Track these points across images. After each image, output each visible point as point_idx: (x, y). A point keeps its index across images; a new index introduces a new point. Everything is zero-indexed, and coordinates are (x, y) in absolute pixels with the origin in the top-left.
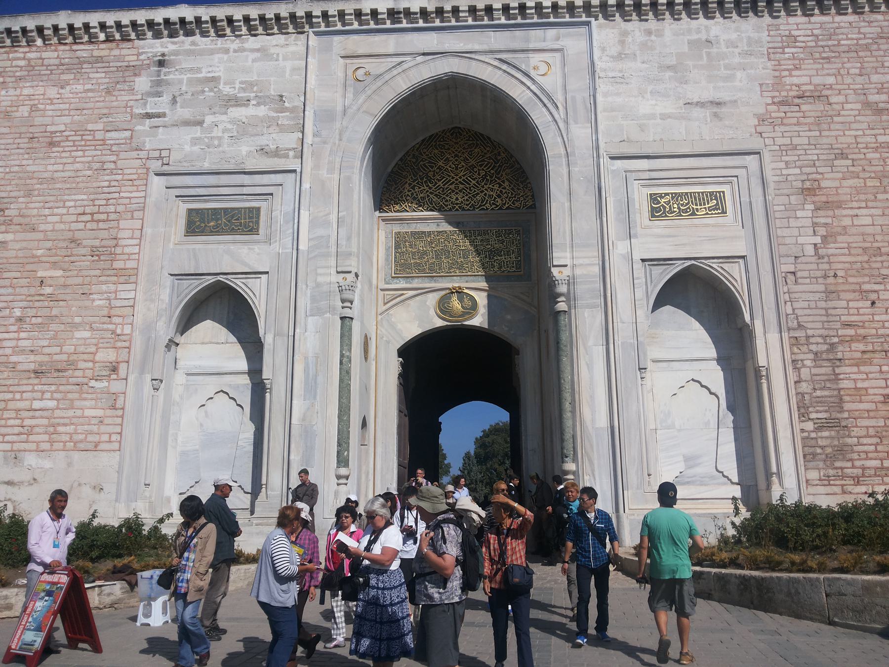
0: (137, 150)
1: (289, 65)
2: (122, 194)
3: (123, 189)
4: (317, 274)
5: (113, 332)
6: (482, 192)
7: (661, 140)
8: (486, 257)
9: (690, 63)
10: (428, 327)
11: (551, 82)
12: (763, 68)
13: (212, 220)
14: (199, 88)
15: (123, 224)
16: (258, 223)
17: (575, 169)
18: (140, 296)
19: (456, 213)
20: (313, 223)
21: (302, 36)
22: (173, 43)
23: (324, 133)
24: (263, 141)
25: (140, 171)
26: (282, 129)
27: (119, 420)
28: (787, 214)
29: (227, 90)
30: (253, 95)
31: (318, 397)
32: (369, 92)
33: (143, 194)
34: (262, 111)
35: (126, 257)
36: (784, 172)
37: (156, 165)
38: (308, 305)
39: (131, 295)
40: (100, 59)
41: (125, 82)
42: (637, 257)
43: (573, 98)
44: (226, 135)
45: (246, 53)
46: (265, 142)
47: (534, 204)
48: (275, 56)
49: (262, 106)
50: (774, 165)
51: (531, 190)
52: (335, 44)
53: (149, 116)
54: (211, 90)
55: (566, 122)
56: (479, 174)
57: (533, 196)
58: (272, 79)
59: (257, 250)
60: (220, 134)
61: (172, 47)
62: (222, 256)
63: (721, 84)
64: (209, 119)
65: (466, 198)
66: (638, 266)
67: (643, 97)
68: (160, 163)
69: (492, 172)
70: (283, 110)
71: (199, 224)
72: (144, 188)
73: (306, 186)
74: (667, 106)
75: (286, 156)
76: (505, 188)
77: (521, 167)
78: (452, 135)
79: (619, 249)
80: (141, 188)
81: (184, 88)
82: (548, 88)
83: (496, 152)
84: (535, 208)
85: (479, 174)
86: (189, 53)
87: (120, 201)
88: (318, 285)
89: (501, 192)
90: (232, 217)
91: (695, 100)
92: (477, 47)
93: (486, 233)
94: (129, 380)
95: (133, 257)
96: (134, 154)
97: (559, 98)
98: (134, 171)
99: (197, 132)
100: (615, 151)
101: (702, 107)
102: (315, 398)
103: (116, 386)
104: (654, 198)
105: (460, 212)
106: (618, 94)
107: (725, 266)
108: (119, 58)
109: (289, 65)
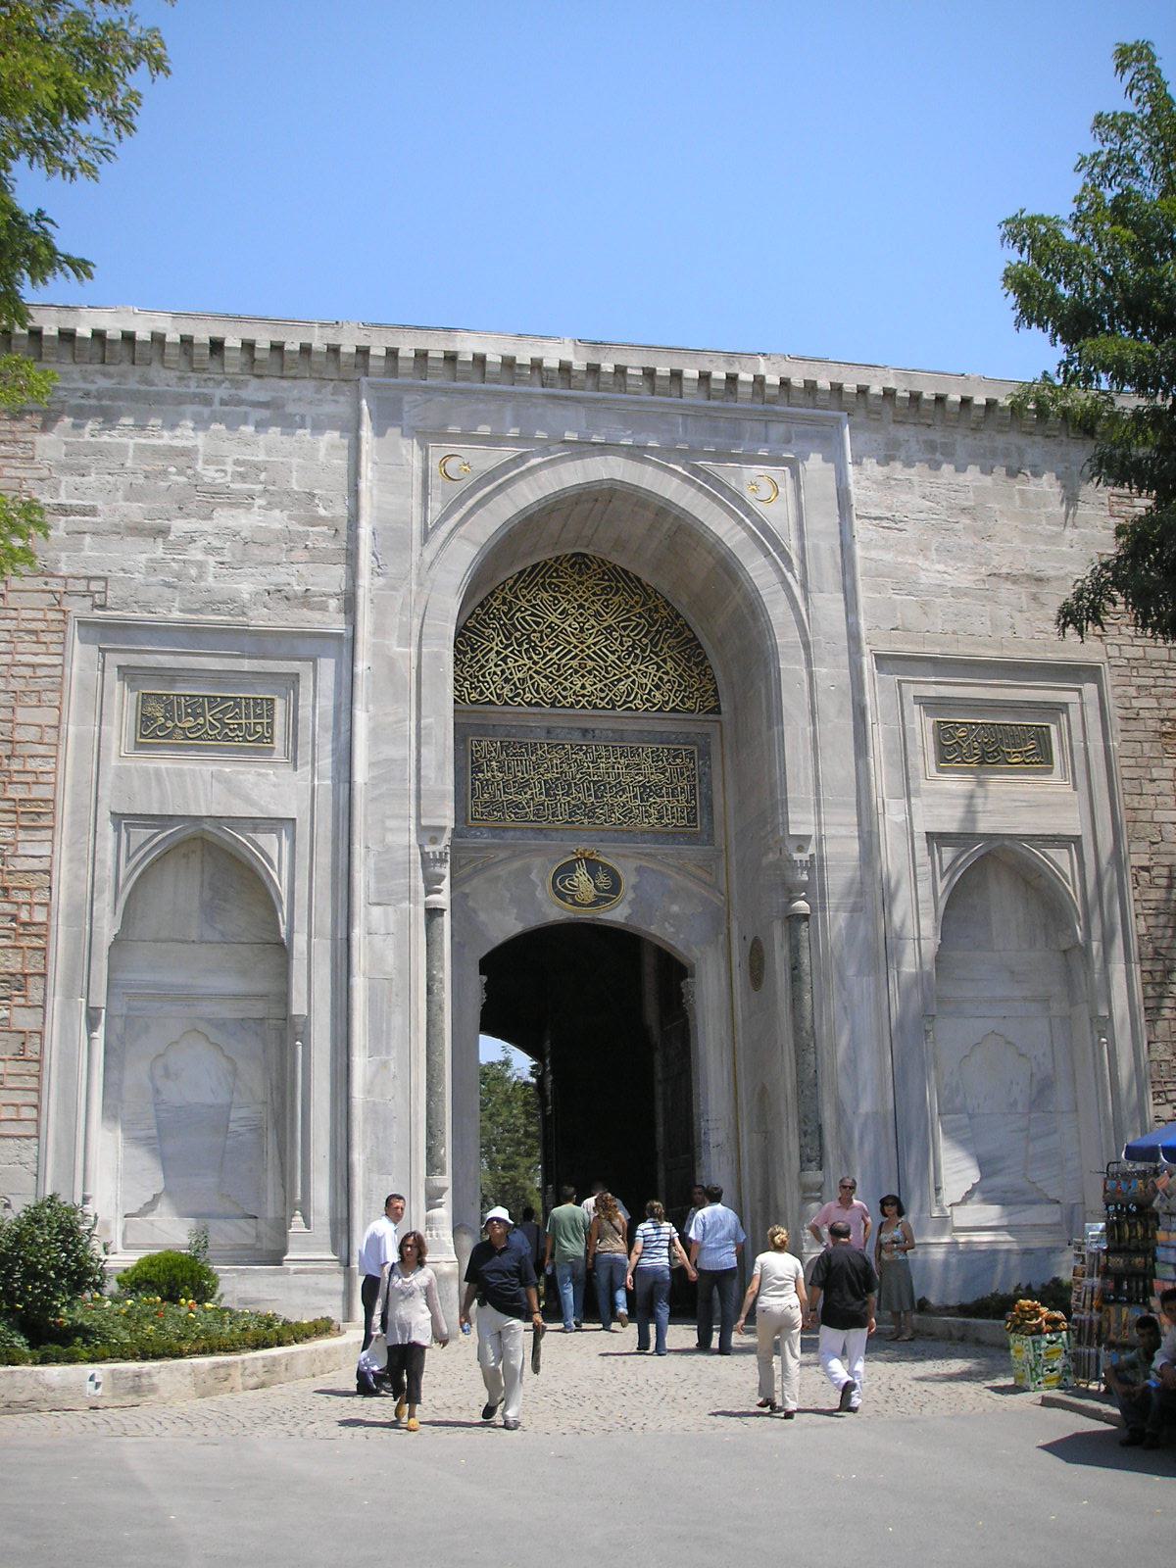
0: (42, 574)
2: (18, 657)
3: (20, 647)
4: (386, 829)
5: (14, 918)
6: (628, 676)
7: (954, 633)
8: (635, 797)
9: (997, 507)
10: (533, 922)
11: (778, 513)
12: (1104, 528)
13: (188, 715)
14: (159, 465)
15: (22, 715)
16: (270, 725)
17: (820, 671)
18: (63, 855)
19: (584, 712)
20: (375, 735)
21: (346, 387)
22: (106, 375)
23: (391, 570)
24: (279, 576)
25: (51, 615)
26: (317, 558)
27: (32, 1083)
28: (1139, 772)
29: (210, 474)
30: (260, 487)
31: (394, 1053)
32: (471, 502)
33: (56, 660)
34: (278, 520)
35: (30, 778)
36: (1136, 703)
37: (78, 608)
38: (372, 885)
39: (45, 850)
41: (16, 442)
42: (920, 828)
43: (816, 547)
44: (211, 560)
45: (244, 409)
46: (284, 579)
47: (719, 706)
48: (297, 418)
49: (276, 512)
50: (1119, 691)
51: (713, 679)
52: (406, 409)
54: (180, 473)
55: (804, 586)
56: (621, 644)
57: (716, 690)
58: (295, 461)
59: (273, 779)
60: (200, 557)
61: (103, 383)
62: (204, 784)
63: (1043, 548)
64: (179, 526)
65: (599, 686)
66: (921, 844)
67: (926, 558)
68: (88, 602)
70: (316, 520)
72: (58, 649)
73: (361, 667)
74: (961, 577)
75: (323, 608)
76: (667, 673)
77: (695, 638)
78: (572, 567)
79: (892, 815)
80: (54, 648)
81: (129, 464)
82: (774, 525)
83: (651, 605)
84: (719, 713)
85: (621, 644)
87: (16, 671)
88: (388, 849)
89: (661, 679)
90: (223, 712)
91: (1004, 570)
93: (635, 753)
94: (49, 1008)
95: (43, 778)
96: (38, 583)
97: (792, 545)
98: (40, 615)
100: (884, 648)
101: (1014, 583)
102: (388, 1053)
103: (24, 1020)
104: (943, 731)
105: (590, 711)
106: (886, 548)
107: (1050, 852)
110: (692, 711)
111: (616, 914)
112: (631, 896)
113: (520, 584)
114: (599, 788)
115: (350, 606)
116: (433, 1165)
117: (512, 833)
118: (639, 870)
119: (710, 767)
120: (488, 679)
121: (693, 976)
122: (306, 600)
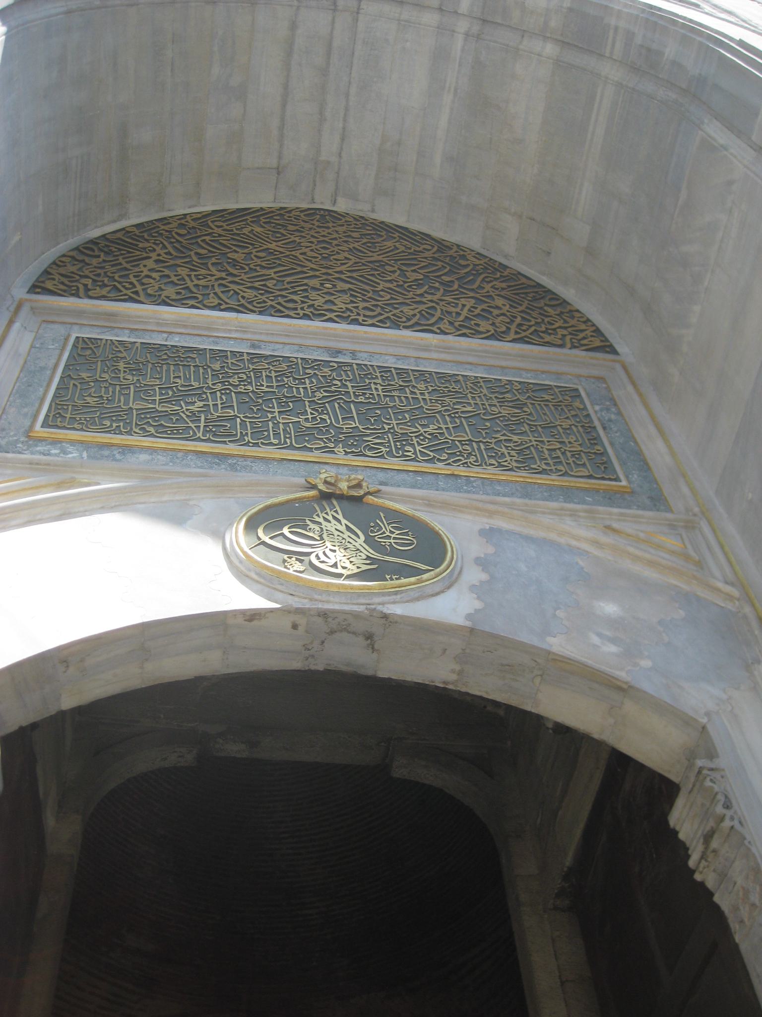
69: (446, 278)
110: (561, 346)
112: (473, 575)
113: (212, 218)
117: (144, 457)
118: (488, 534)
119: (619, 413)
120: (134, 280)
121: (712, 755)
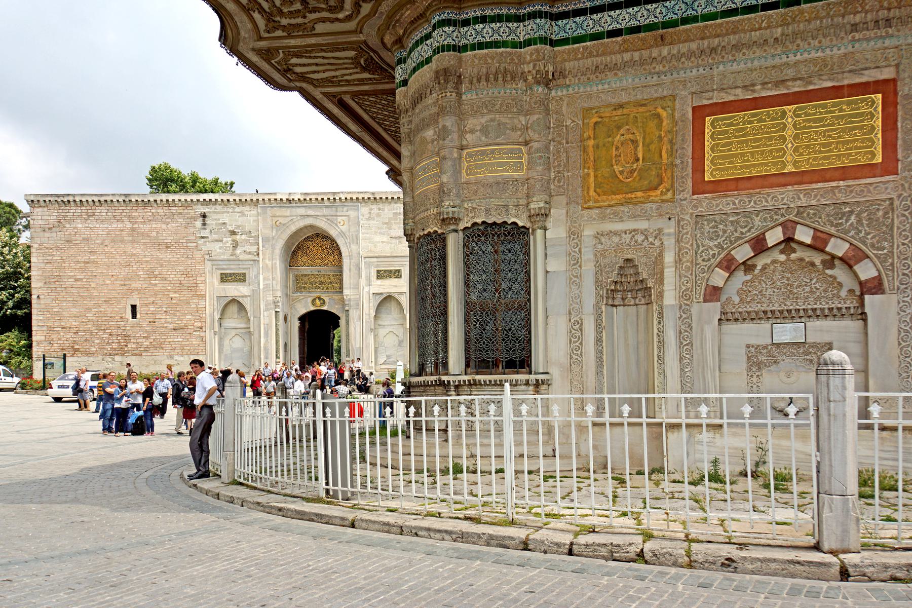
1: (252, 219)
18: (208, 304)
20: (264, 279)
24: (245, 248)
26: (251, 244)
40: (180, 214)
42: (371, 292)
53: (203, 237)
64: (225, 240)
71: (225, 278)
86: (215, 212)
92: (319, 214)
99: (221, 244)
108: (188, 213)
109: (252, 219)
111: (325, 308)
114: (321, 283)
115: (258, 254)
116: (277, 357)
122: (250, 253)
